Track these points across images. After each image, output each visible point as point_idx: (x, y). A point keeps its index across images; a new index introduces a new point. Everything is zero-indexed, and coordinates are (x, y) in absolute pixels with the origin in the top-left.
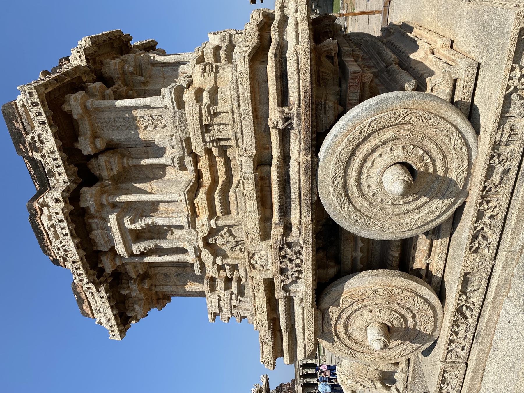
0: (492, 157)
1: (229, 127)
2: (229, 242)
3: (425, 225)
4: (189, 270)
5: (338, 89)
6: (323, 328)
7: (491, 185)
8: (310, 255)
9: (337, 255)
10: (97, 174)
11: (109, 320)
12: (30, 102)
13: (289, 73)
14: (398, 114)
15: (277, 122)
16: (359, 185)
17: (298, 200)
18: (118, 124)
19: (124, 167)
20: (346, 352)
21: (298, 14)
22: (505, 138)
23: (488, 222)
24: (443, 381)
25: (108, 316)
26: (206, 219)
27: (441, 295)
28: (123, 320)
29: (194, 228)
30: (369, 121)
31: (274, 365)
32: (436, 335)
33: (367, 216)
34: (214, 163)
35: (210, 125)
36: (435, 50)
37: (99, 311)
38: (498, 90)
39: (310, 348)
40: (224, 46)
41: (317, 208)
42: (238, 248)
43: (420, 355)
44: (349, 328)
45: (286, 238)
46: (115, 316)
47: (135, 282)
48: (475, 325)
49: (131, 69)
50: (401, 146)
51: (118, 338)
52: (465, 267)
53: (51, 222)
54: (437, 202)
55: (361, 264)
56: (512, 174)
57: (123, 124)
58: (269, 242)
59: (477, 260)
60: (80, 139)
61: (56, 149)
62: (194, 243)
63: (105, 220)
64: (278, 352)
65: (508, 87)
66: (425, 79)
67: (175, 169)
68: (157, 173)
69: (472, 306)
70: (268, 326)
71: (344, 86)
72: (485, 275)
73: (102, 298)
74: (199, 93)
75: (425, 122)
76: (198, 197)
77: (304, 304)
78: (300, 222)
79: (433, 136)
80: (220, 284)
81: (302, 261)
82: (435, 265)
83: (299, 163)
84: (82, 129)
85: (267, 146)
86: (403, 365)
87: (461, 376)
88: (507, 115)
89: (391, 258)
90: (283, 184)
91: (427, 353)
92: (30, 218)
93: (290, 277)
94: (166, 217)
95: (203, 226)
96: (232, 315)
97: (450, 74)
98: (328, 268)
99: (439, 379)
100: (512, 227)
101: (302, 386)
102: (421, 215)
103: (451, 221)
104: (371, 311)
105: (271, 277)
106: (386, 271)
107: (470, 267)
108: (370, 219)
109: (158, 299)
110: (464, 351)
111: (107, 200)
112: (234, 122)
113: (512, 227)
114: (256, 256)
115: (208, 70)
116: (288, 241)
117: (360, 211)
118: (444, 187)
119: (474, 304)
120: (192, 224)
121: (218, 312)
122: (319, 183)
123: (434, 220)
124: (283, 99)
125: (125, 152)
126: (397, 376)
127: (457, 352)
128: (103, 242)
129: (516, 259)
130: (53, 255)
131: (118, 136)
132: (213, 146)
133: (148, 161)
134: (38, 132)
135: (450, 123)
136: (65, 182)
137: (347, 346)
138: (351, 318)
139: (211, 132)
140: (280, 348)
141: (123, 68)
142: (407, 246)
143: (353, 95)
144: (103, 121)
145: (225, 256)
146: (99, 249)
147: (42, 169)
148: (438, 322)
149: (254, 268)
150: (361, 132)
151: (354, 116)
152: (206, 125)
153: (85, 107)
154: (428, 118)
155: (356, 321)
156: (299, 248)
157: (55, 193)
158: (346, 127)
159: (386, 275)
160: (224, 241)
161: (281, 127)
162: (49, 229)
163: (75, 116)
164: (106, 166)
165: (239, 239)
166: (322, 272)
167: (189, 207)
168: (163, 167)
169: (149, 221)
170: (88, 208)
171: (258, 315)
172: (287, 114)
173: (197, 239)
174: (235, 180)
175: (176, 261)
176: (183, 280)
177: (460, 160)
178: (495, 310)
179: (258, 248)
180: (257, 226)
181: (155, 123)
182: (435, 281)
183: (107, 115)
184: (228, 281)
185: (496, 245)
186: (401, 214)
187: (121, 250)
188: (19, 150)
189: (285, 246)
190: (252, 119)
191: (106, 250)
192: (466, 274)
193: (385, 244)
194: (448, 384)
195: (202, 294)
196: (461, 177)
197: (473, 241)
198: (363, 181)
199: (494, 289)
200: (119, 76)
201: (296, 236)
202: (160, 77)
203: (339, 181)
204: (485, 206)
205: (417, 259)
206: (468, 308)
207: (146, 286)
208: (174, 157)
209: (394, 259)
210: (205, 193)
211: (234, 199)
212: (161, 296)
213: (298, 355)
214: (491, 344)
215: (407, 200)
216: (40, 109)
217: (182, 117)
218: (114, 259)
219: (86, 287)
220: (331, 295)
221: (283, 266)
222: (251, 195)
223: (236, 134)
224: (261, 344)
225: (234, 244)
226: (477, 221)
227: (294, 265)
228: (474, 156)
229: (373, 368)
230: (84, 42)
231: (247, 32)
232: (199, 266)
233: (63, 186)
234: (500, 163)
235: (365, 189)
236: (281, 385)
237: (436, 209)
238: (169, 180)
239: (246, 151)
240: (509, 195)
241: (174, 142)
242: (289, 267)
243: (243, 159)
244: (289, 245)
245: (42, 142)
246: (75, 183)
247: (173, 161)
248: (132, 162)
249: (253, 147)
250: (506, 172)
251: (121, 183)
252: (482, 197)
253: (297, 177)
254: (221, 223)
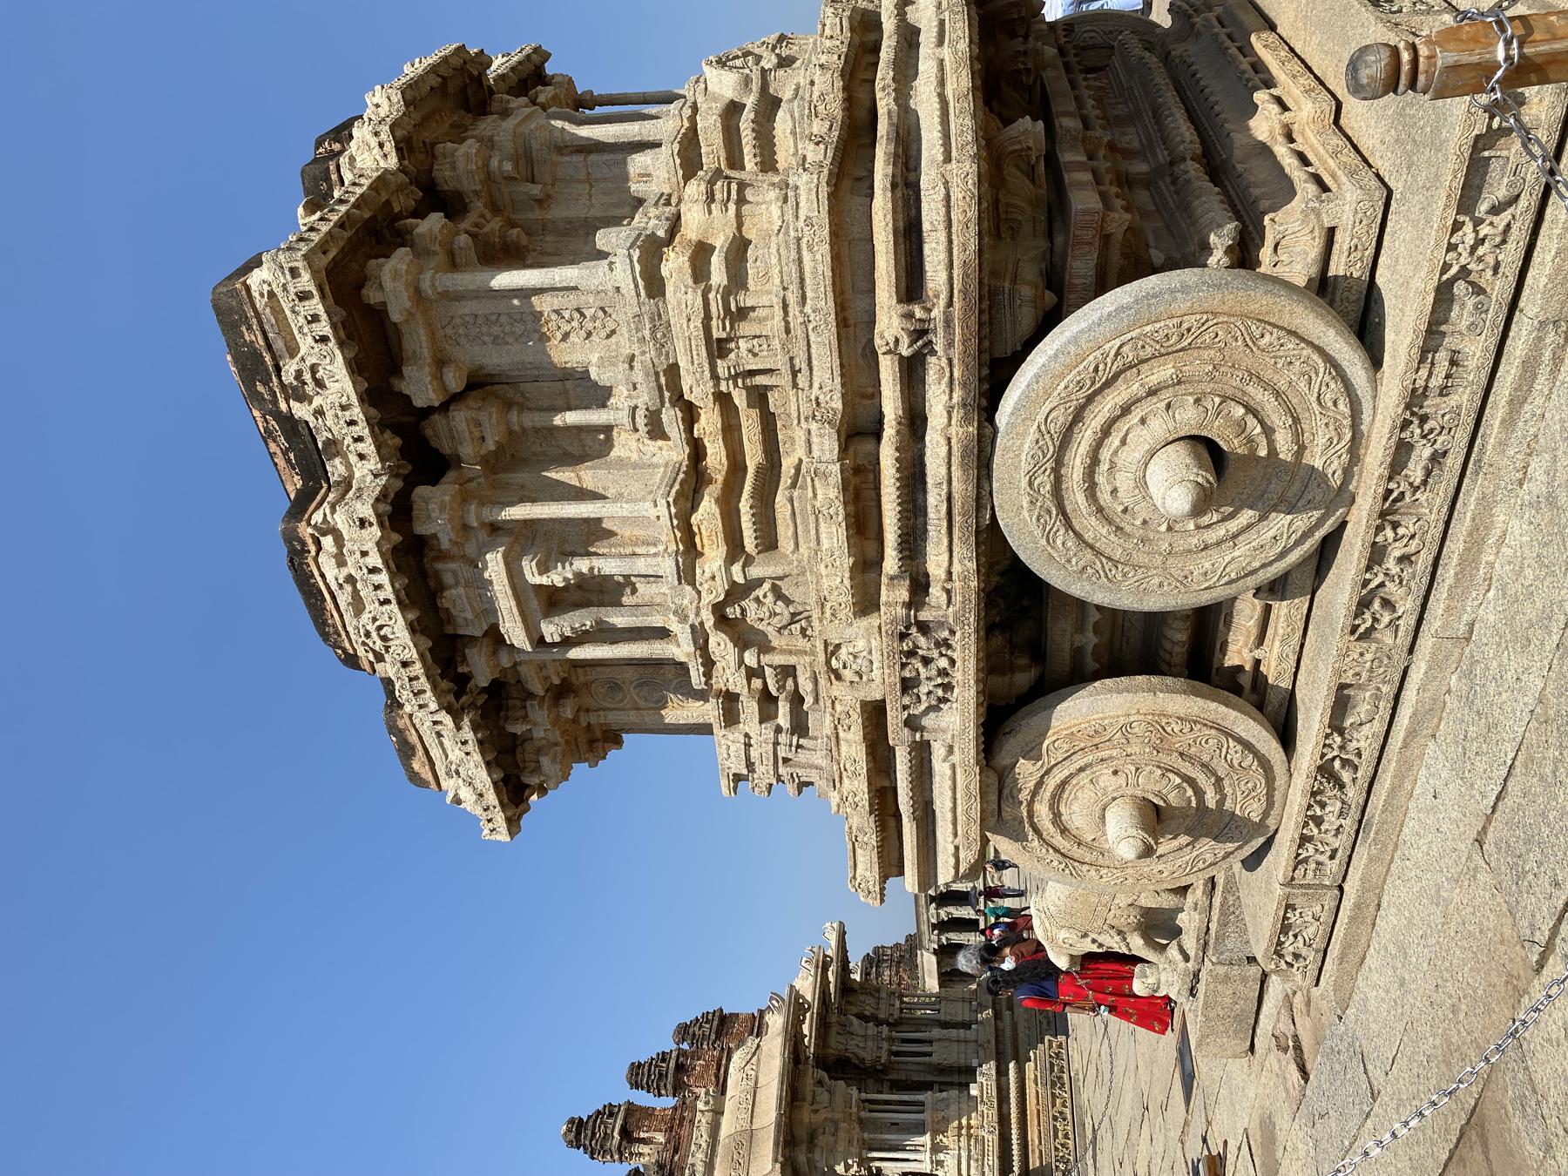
0: (1406, 424)
1: (776, 344)
2: (776, 614)
3: (1246, 575)
4: (670, 673)
5: (1043, 244)
6: (1000, 806)
7: (1404, 486)
8: (973, 649)
9: (1034, 644)
10: (446, 449)
11: (481, 795)
12: (292, 290)
13: (926, 226)
14: (1185, 326)
15: (897, 341)
16: (1091, 490)
17: (945, 524)
18: (496, 330)
19: (511, 432)
20: (1055, 863)
21: (946, 52)
22: (1436, 382)
23: (1395, 570)
24: (1285, 928)
25: (479, 786)
26: (720, 562)
27: (1286, 736)
28: (514, 792)
29: (692, 582)
30: (1118, 342)
31: (882, 895)
32: (1271, 822)
33: (1109, 559)
34: (733, 422)
35: (729, 340)
36: (1295, 128)
37: (457, 773)
38: (1423, 274)
39: (968, 857)
40: (750, 101)
41: (991, 543)
42: (796, 628)
43: (1237, 867)
44: (1062, 809)
45: (917, 611)
46: (495, 784)
47: (541, 706)
48: (1361, 801)
49: (508, 167)
50: (1191, 399)
51: (503, 836)
52: (1339, 673)
53: (345, 572)
54: (1280, 522)
55: (1096, 660)
56: (1453, 462)
57: (507, 329)
58: (873, 620)
59: (1369, 657)
60: (407, 370)
61: (354, 399)
62: (692, 616)
63: (475, 564)
64: (891, 864)
65: (1446, 267)
66: (1264, 213)
67: (637, 436)
68: (591, 445)
69: (1356, 760)
70: (871, 805)
71: (1059, 239)
72: (1388, 690)
73: (464, 743)
74: (701, 253)
75: (1251, 343)
76: (701, 509)
77: (956, 758)
78: (950, 573)
79: (1268, 375)
80: (749, 708)
81: (953, 662)
82: (1273, 664)
83: (949, 440)
84: (409, 345)
85: (870, 390)
86: (1197, 894)
87: (1326, 917)
88: (1443, 328)
89: (1168, 646)
90: (908, 486)
91: (1253, 862)
92: (291, 561)
93: (924, 698)
94: (621, 556)
95: (713, 578)
96: (779, 779)
97: (1318, 215)
98: (1013, 672)
99: (1274, 925)
100: (1448, 582)
101: (935, 952)
102: (1237, 553)
103: (1314, 562)
104: (1115, 773)
105: (879, 697)
106: (1155, 679)
107: (1351, 673)
108: (1116, 563)
109: (592, 742)
110: (1336, 861)
111: (478, 517)
112: (788, 331)
113: (1448, 582)
114: (843, 651)
115: (718, 196)
116: (921, 618)
117: (1092, 547)
118: (1294, 488)
119: (1359, 755)
120: (687, 574)
121: (745, 772)
122: (995, 485)
123: (1271, 563)
124: (911, 286)
125: (511, 393)
126: (1182, 920)
127: (1318, 863)
129: (1457, 652)
130: (347, 645)
131: (495, 359)
132: (736, 385)
133: (572, 418)
134: (310, 361)
135: (1310, 344)
136: (376, 476)
137: (1057, 850)
138: (1068, 788)
139: (732, 356)
140: (896, 855)
141: (486, 165)
142: (1208, 623)
143: (1081, 267)
144: (458, 321)
145: (765, 647)
146: (461, 632)
147: (308, 439)
148: (1278, 796)
149: (839, 677)
150: (1096, 370)
151: (1082, 331)
152: (719, 340)
153: (418, 292)
154: (1257, 334)
155: (1079, 794)
156: (946, 634)
157: (358, 505)
158: (1062, 358)
159: (1153, 690)
160: (764, 612)
161: (905, 351)
162: (341, 586)
163: (395, 316)
164: (470, 433)
165: (800, 609)
166: (999, 681)
167: (679, 535)
168: (608, 429)
169: (582, 565)
170: (435, 536)
171: (845, 780)
172: (920, 320)
173: (698, 608)
174: (788, 465)
175: (645, 655)
176: (656, 696)
177: (1332, 427)
178: (1406, 769)
179: (849, 632)
180: (847, 582)
181: (589, 325)
182: (1273, 700)
183: (468, 307)
184: (767, 701)
185: (1413, 622)
186: (1190, 551)
187: (514, 632)
188: (254, 397)
189: (913, 630)
190: (834, 329)
191: (478, 633)
192: (1342, 687)
193: (1154, 621)
194: (1295, 936)
195: (706, 729)
196: (1334, 467)
197: (1358, 614)
198: (1100, 479)
199: (1406, 721)
200: (479, 187)
201: (939, 607)
202: (580, 181)
203: (1045, 481)
204: (1389, 533)
205: (1232, 648)
206: (1346, 763)
207: (568, 713)
208: (636, 407)
209: (1177, 649)
210: (717, 501)
211: (789, 513)
212: (598, 734)
213: (939, 871)
214: (1396, 845)
215: (1206, 520)
216: (316, 305)
217: (658, 318)
218: (495, 653)
219: (425, 714)
220: (1020, 737)
222: (832, 511)
223: (791, 359)
224: (850, 846)
225: (786, 618)
226: (1369, 568)
227: (934, 672)
228: (1366, 417)
229: (1122, 900)
230: (383, 102)
231: (815, 97)
232: (702, 669)
233: (374, 487)
234: (1424, 437)
235: (1104, 497)
236: (876, 950)
237: (1279, 536)
238: (621, 463)
239: (818, 404)
240: (1445, 510)
241: (638, 376)
242: (923, 675)
243: (814, 426)
244: (924, 628)
245: (320, 384)
246: (397, 476)
247: (634, 419)
248: (531, 420)
249: (837, 396)
250: (1437, 458)
251: (507, 470)
252: (1383, 515)
253: (944, 471)
254: (755, 572)
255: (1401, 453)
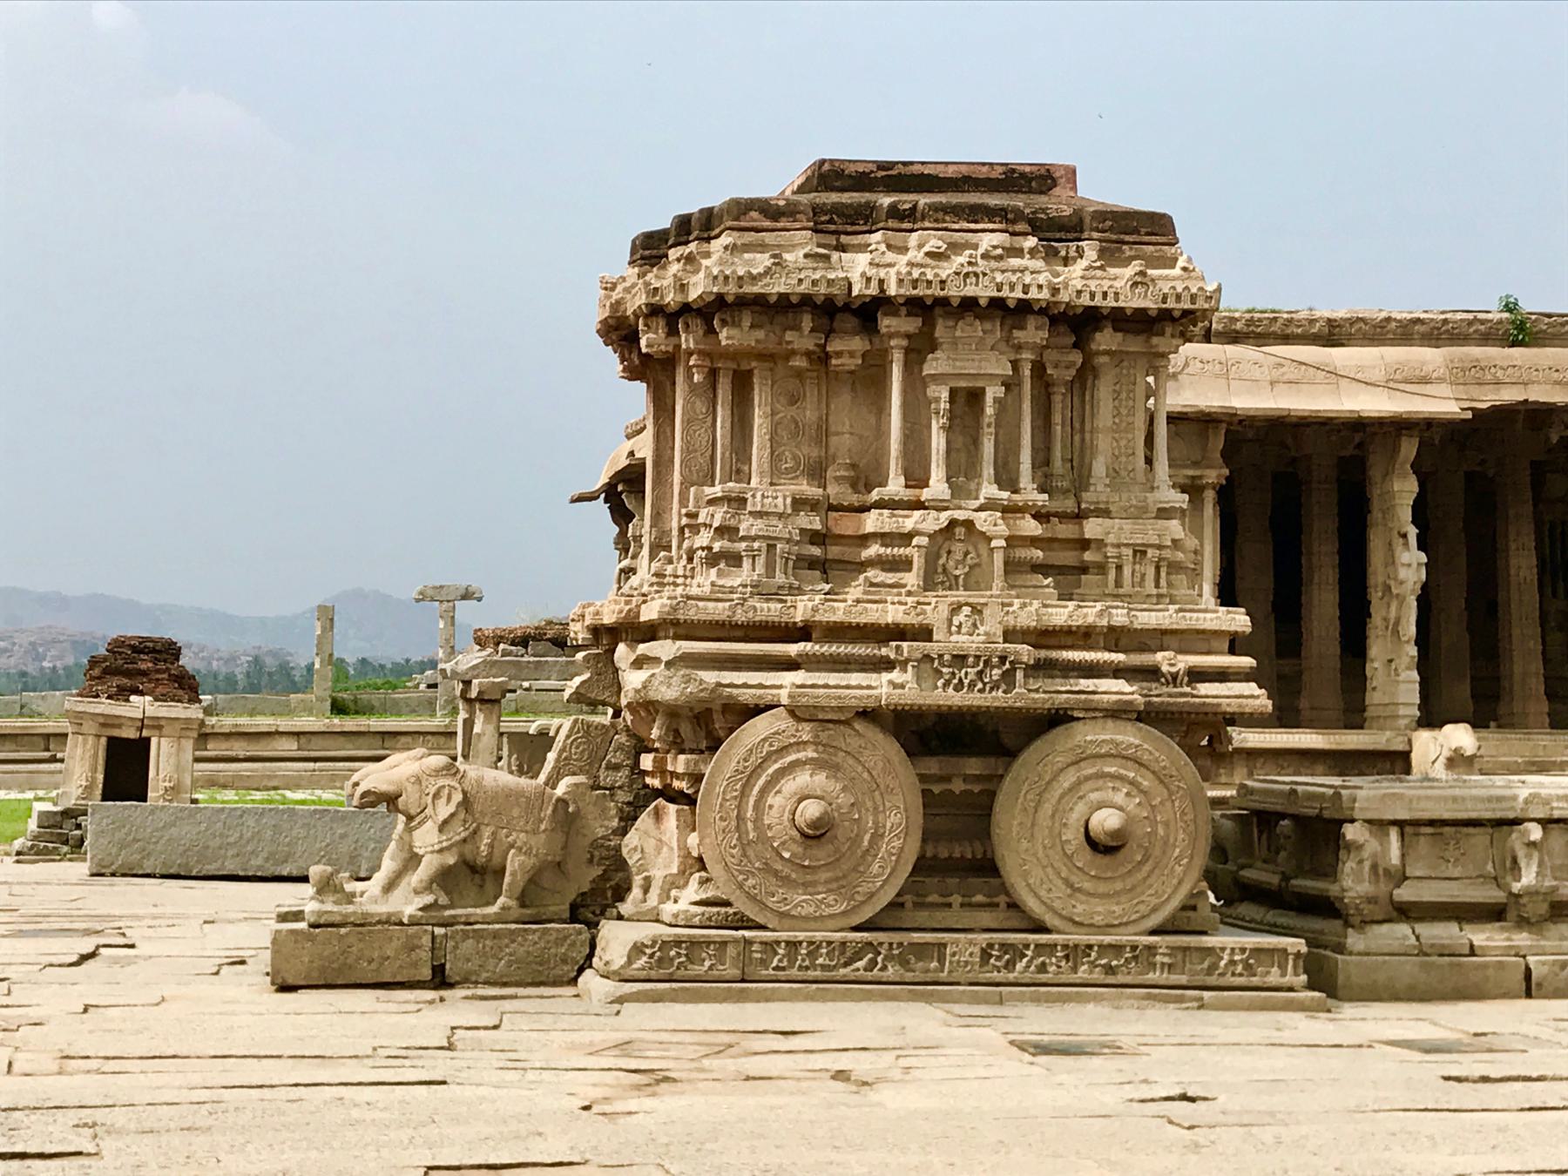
18: (1124, 395)
41: (1057, 719)
56: (1111, 980)
60: (1120, 335)
61: (1122, 304)
105: (935, 637)
124: (1197, 675)
128: (958, 334)
140: (699, 634)
197: (1002, 945)
221: (971, 659)
250: (1110, 970)
255: (1117, 949)
